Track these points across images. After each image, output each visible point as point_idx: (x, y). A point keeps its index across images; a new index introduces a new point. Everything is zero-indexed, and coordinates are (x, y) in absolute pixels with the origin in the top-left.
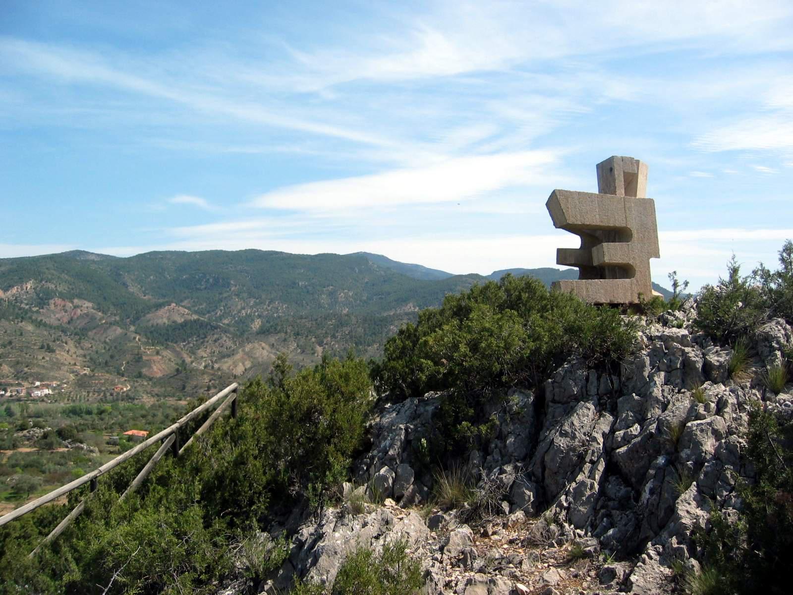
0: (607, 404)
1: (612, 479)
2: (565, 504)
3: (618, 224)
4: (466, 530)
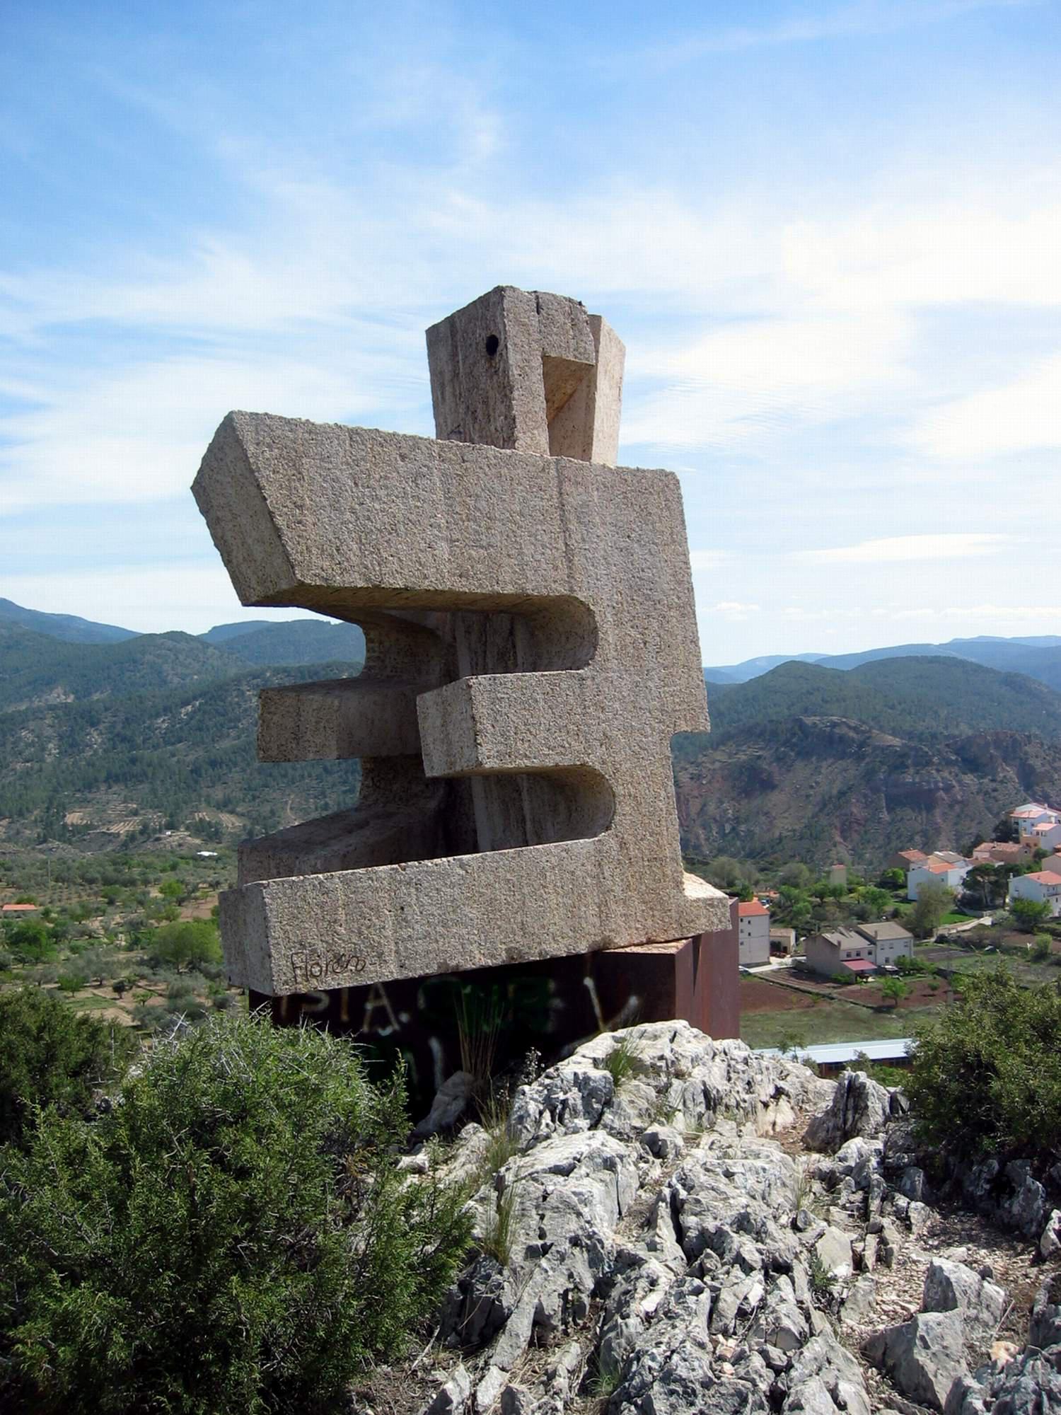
3: (536, 585)
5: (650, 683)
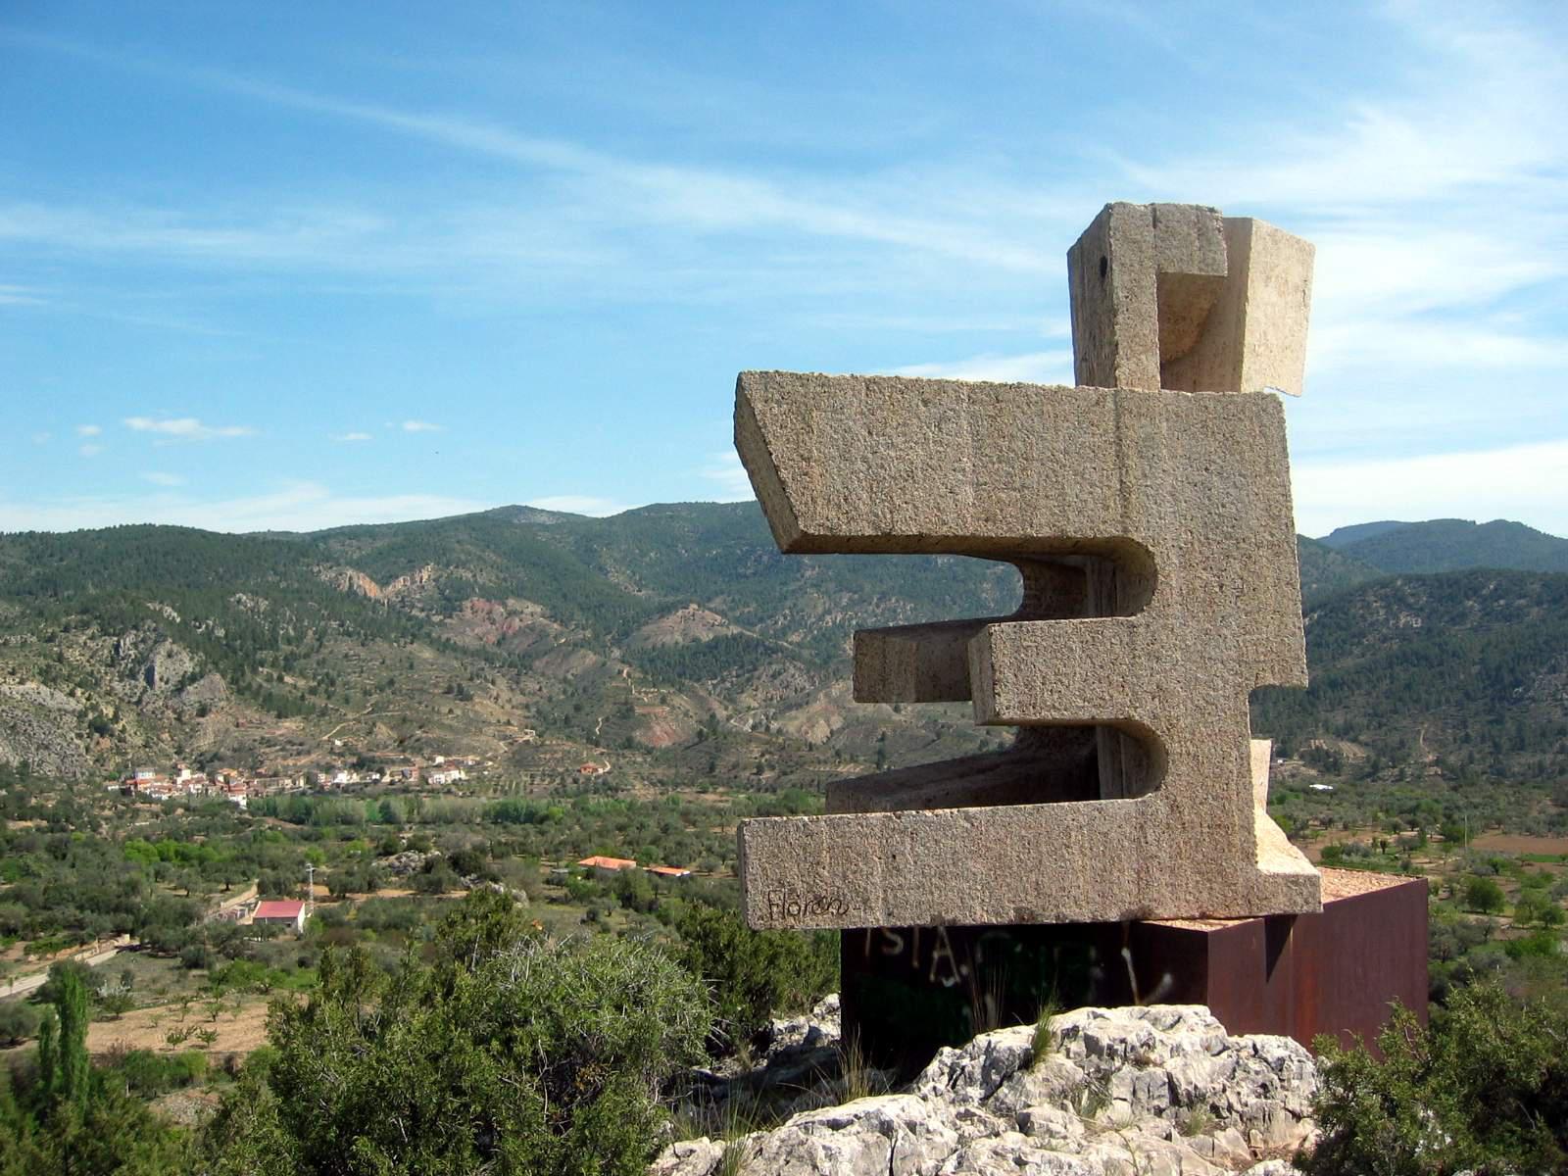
5: (1225, 631)
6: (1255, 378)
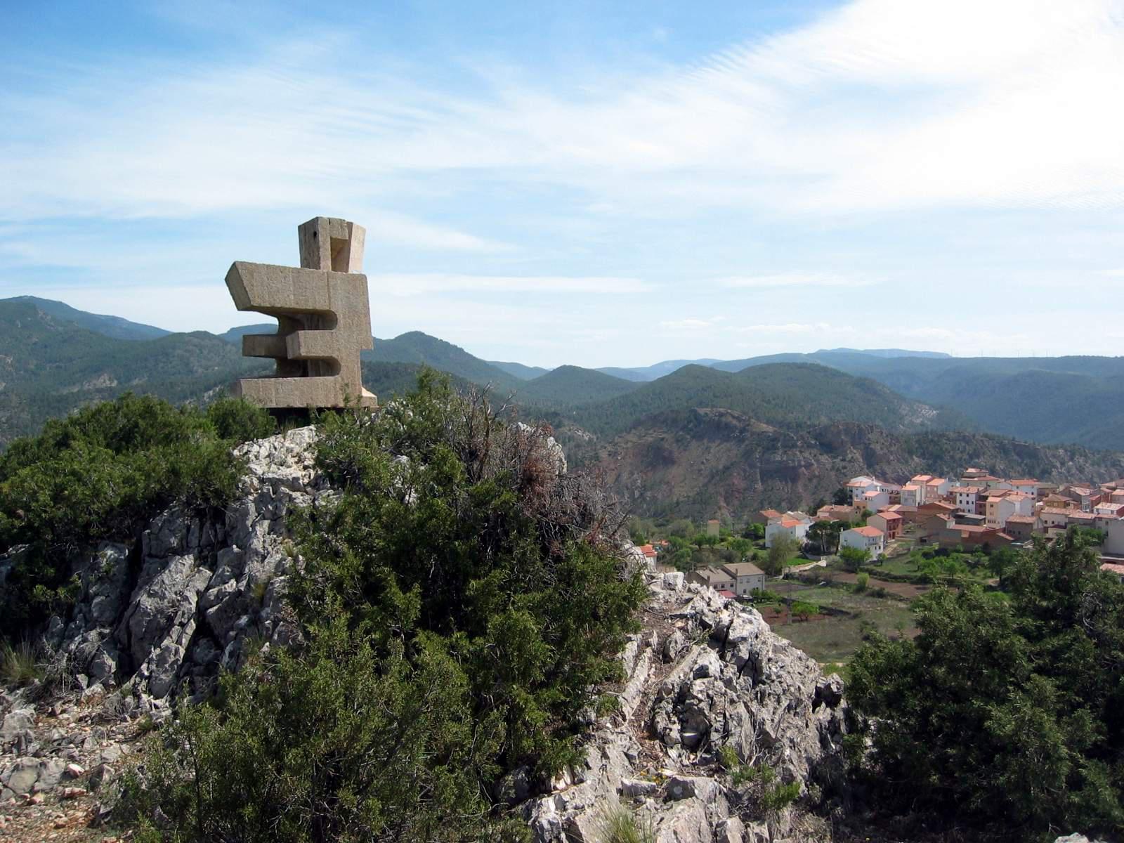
0: (207, 559)
1: (203, 641)
2: (146, 673)
4: (29, 711)
6: (354, 269)
